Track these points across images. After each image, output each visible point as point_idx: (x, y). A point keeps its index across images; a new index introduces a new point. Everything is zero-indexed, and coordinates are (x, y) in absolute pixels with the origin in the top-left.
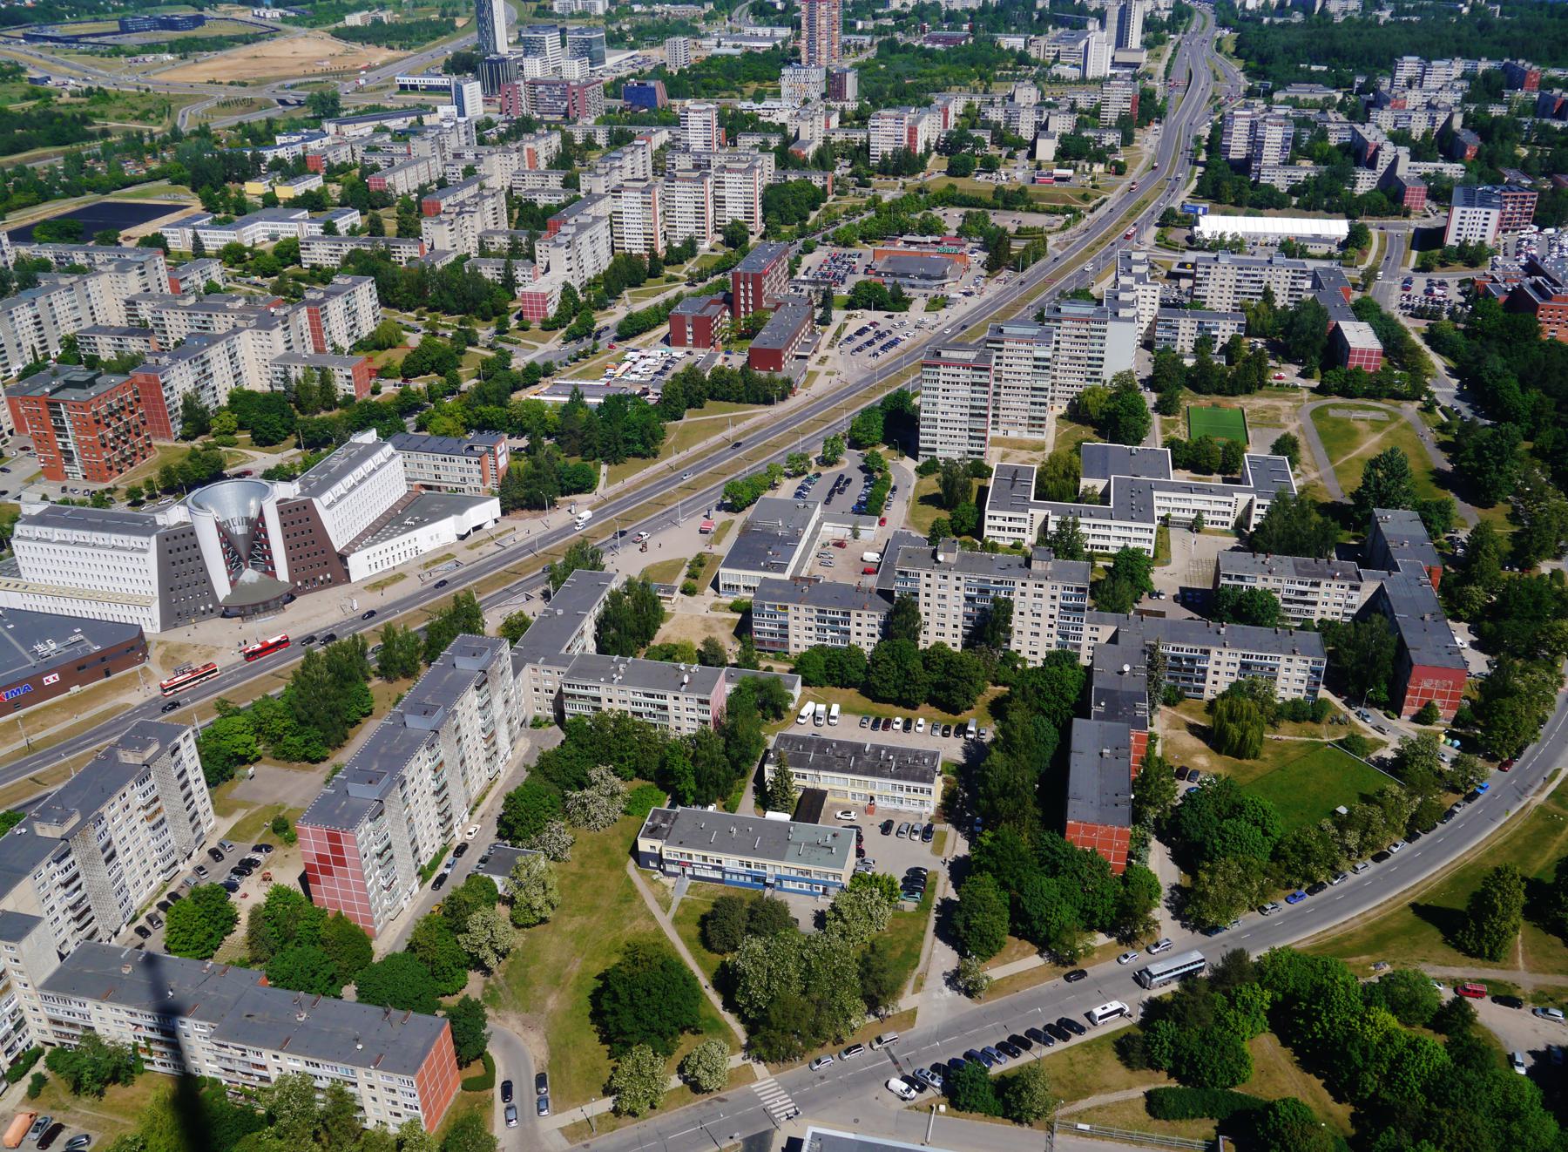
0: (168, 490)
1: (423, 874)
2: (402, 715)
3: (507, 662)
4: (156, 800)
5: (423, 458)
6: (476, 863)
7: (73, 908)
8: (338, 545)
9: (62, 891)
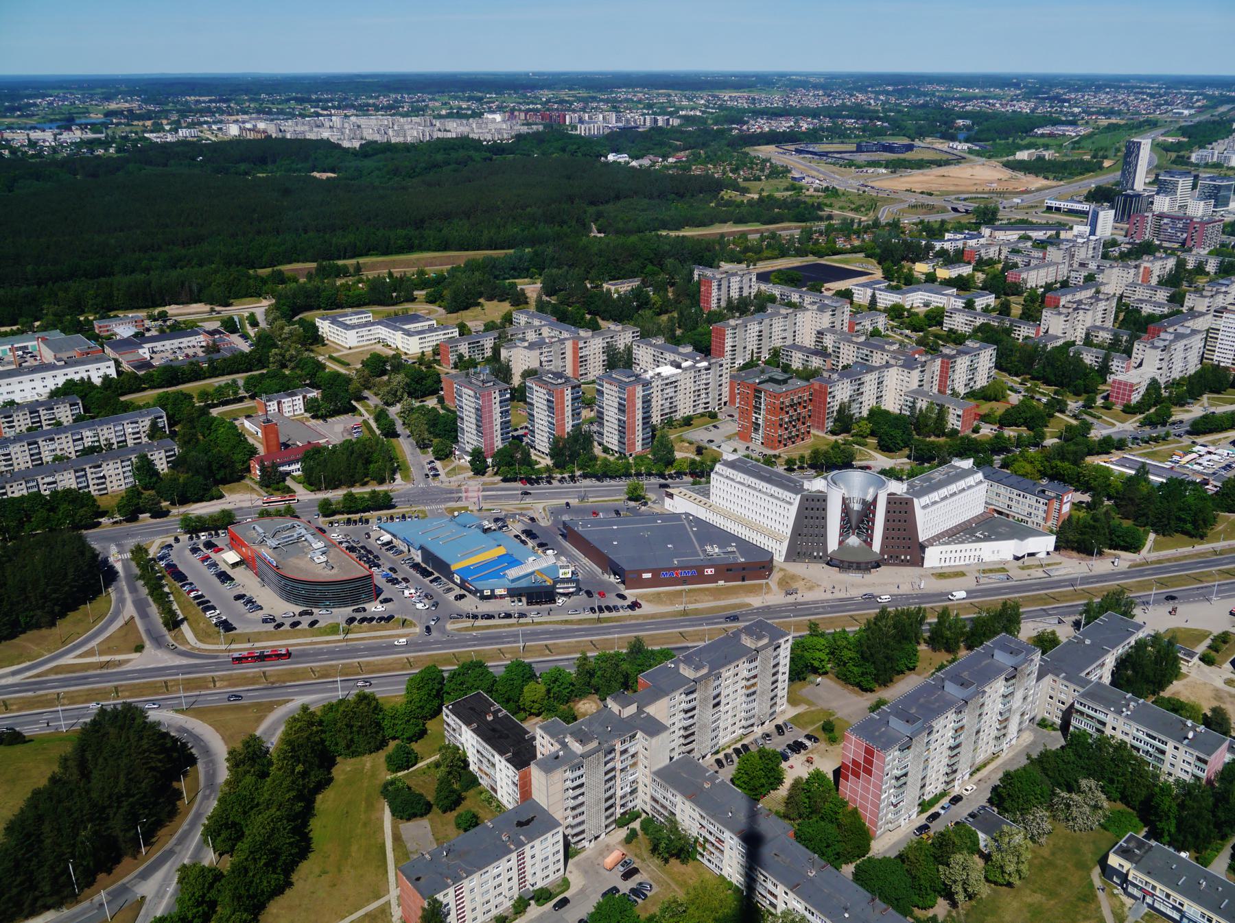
0: (812, 466)
1: (924, 806)
2: (943, 680)
3: (1035, 668)
4: (755, 677)
5: (1002, 490)
6: (966, 815)
7: (686, 729)
8: (922, 537)
9: (682, 715)
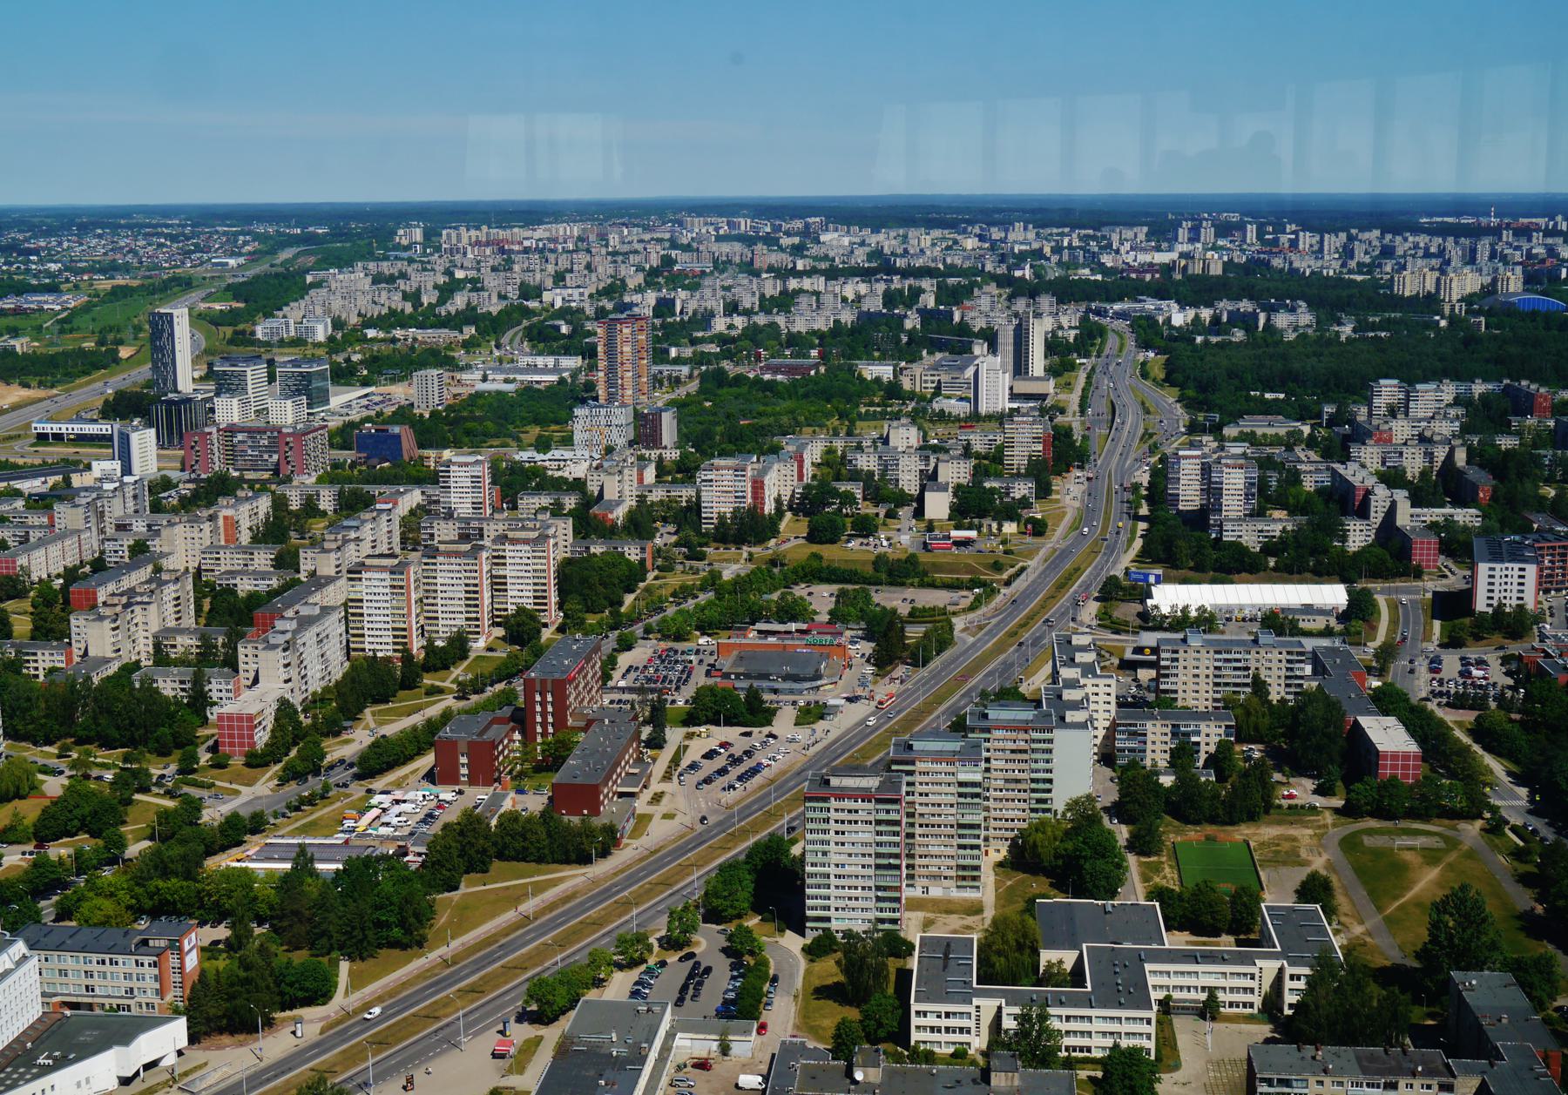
5: (69, 961)
